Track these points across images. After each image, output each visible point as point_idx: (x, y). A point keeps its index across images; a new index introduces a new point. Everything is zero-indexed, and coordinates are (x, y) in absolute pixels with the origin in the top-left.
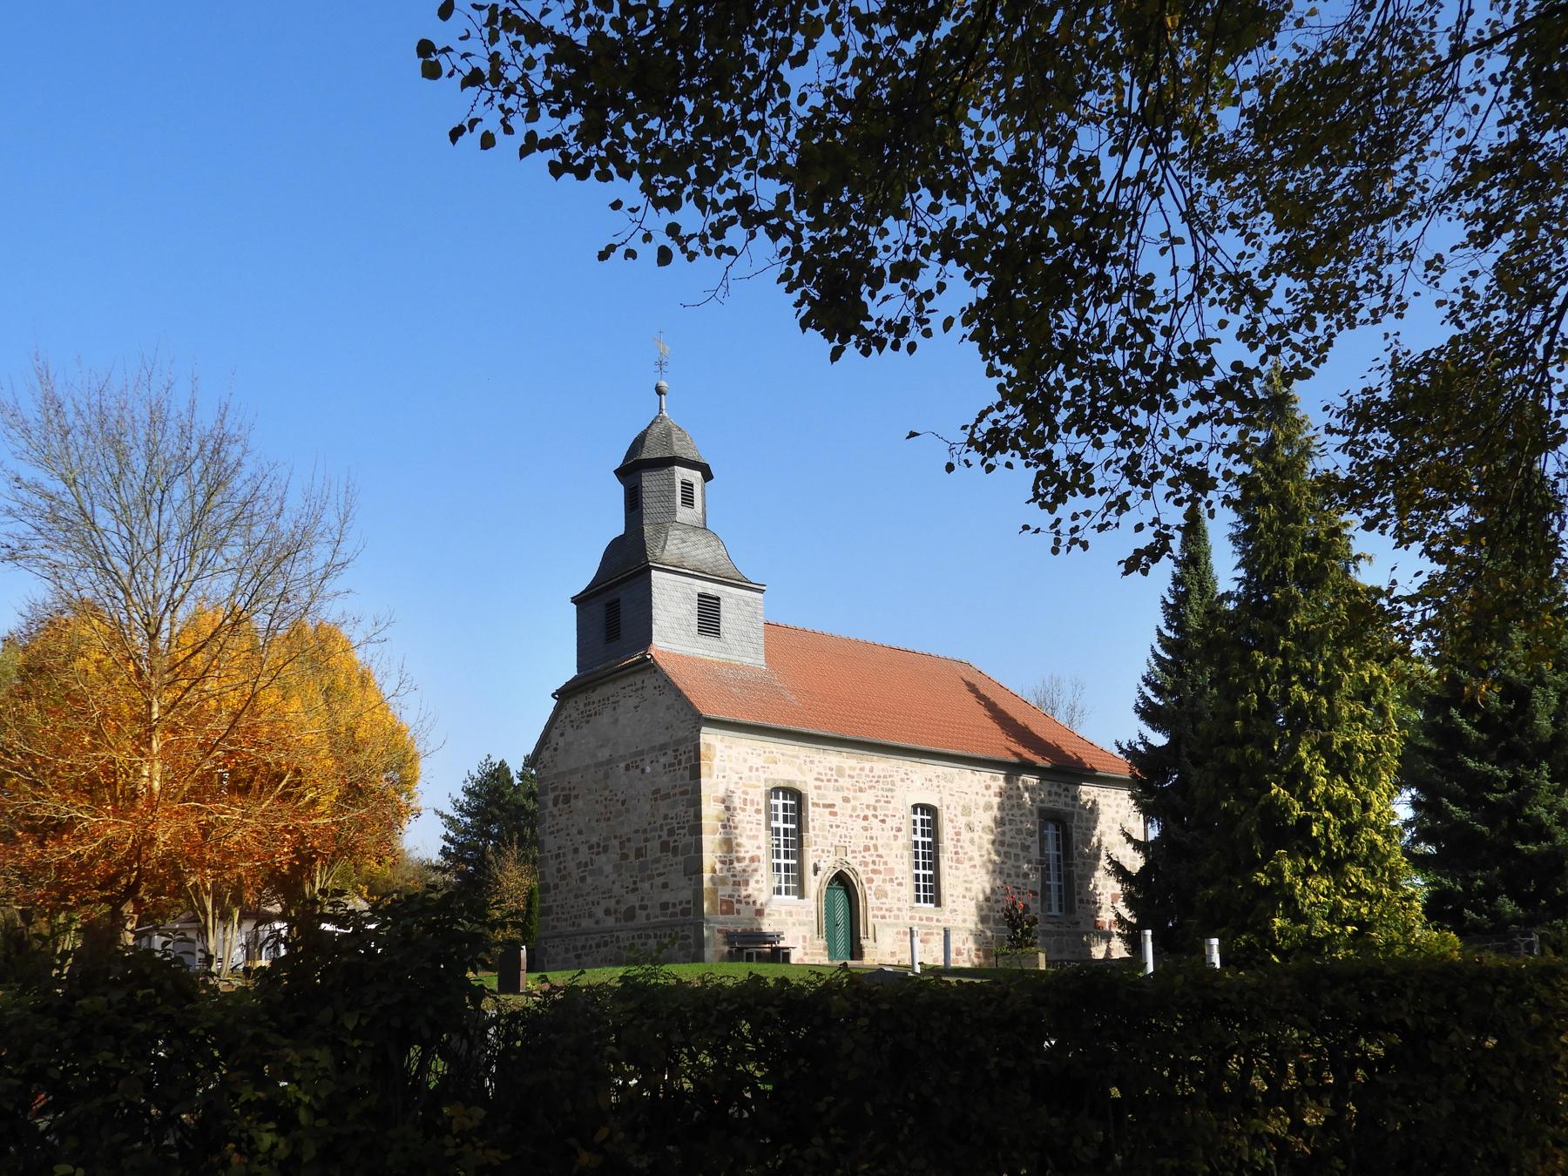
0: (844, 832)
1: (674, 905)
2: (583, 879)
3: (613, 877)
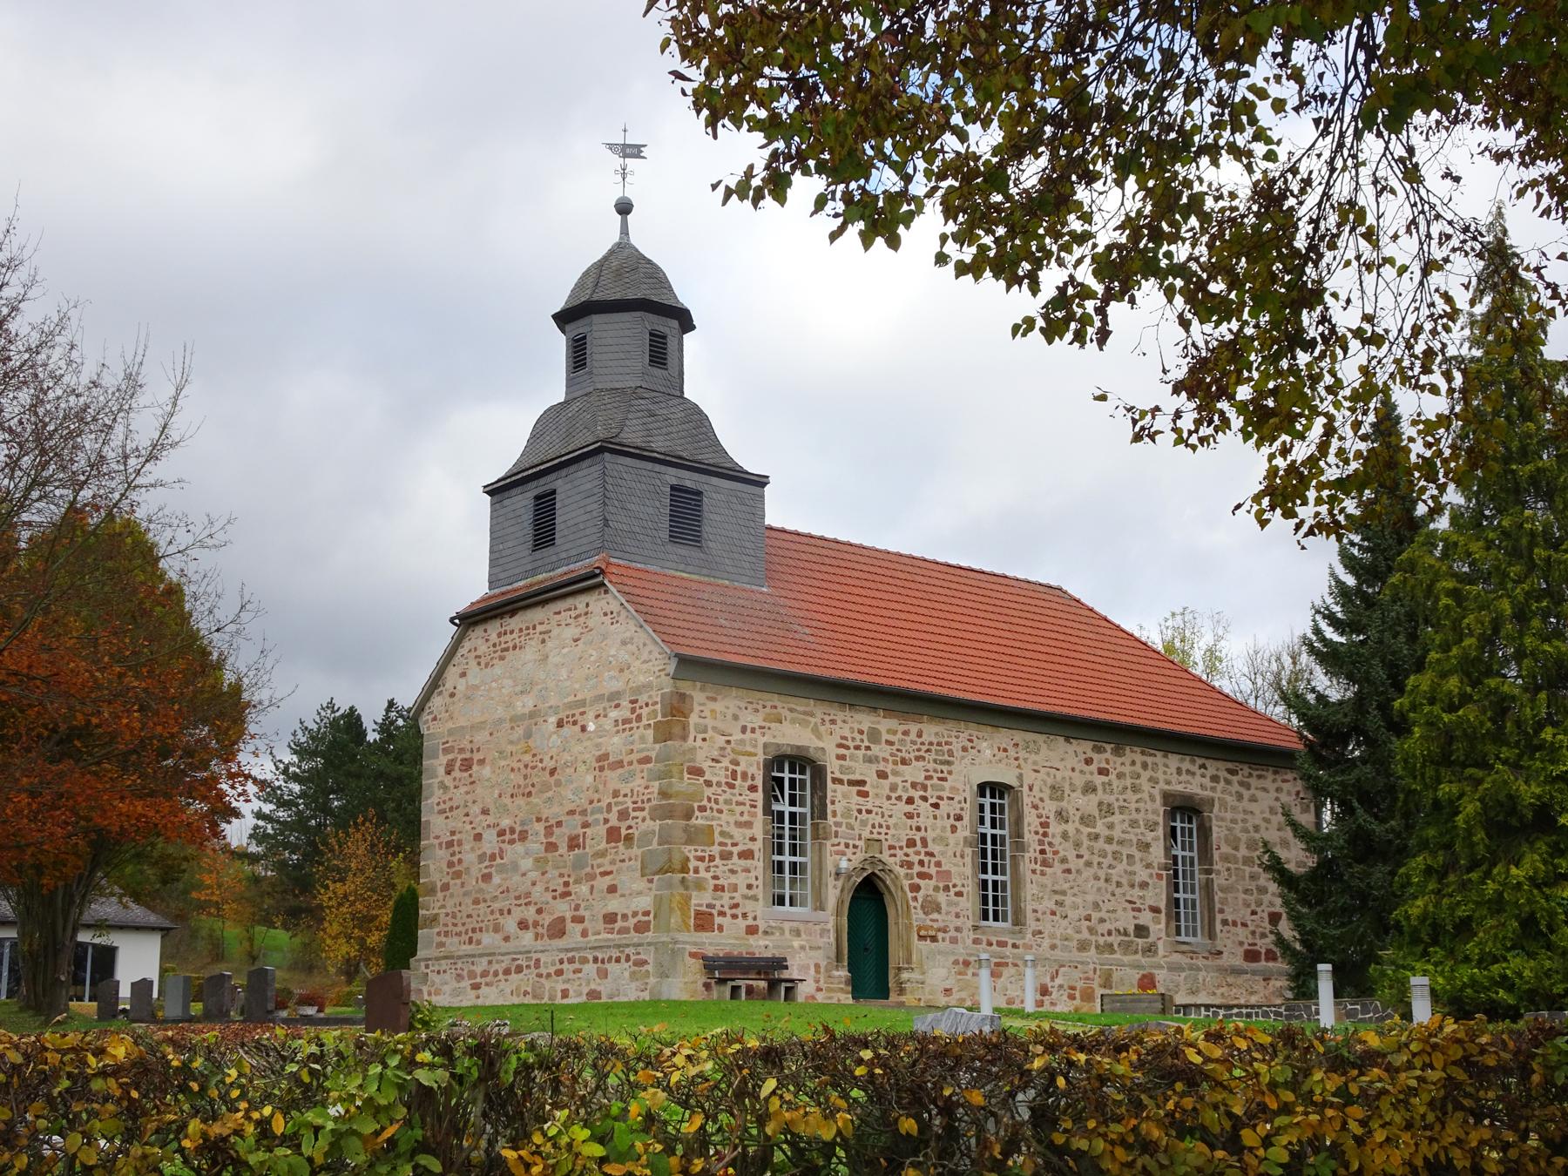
0: (878, 819)
1: (625, 916)
2: (487, 878)
3: (534, 875)
